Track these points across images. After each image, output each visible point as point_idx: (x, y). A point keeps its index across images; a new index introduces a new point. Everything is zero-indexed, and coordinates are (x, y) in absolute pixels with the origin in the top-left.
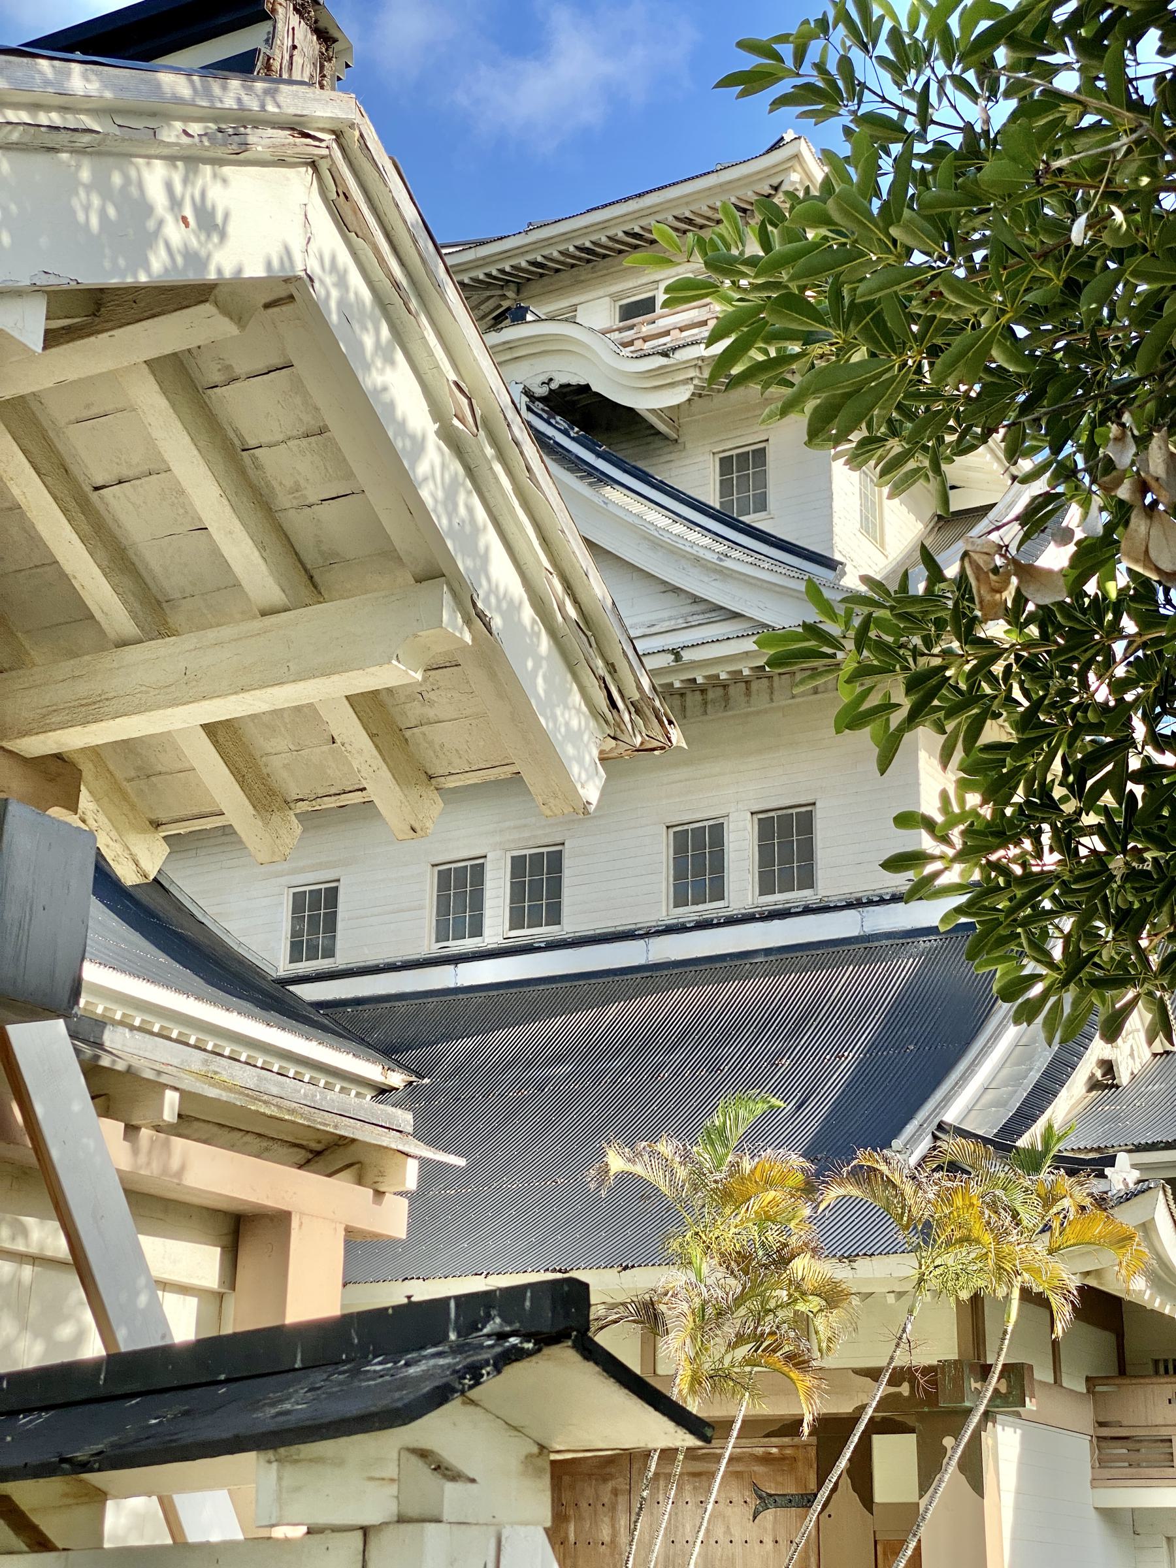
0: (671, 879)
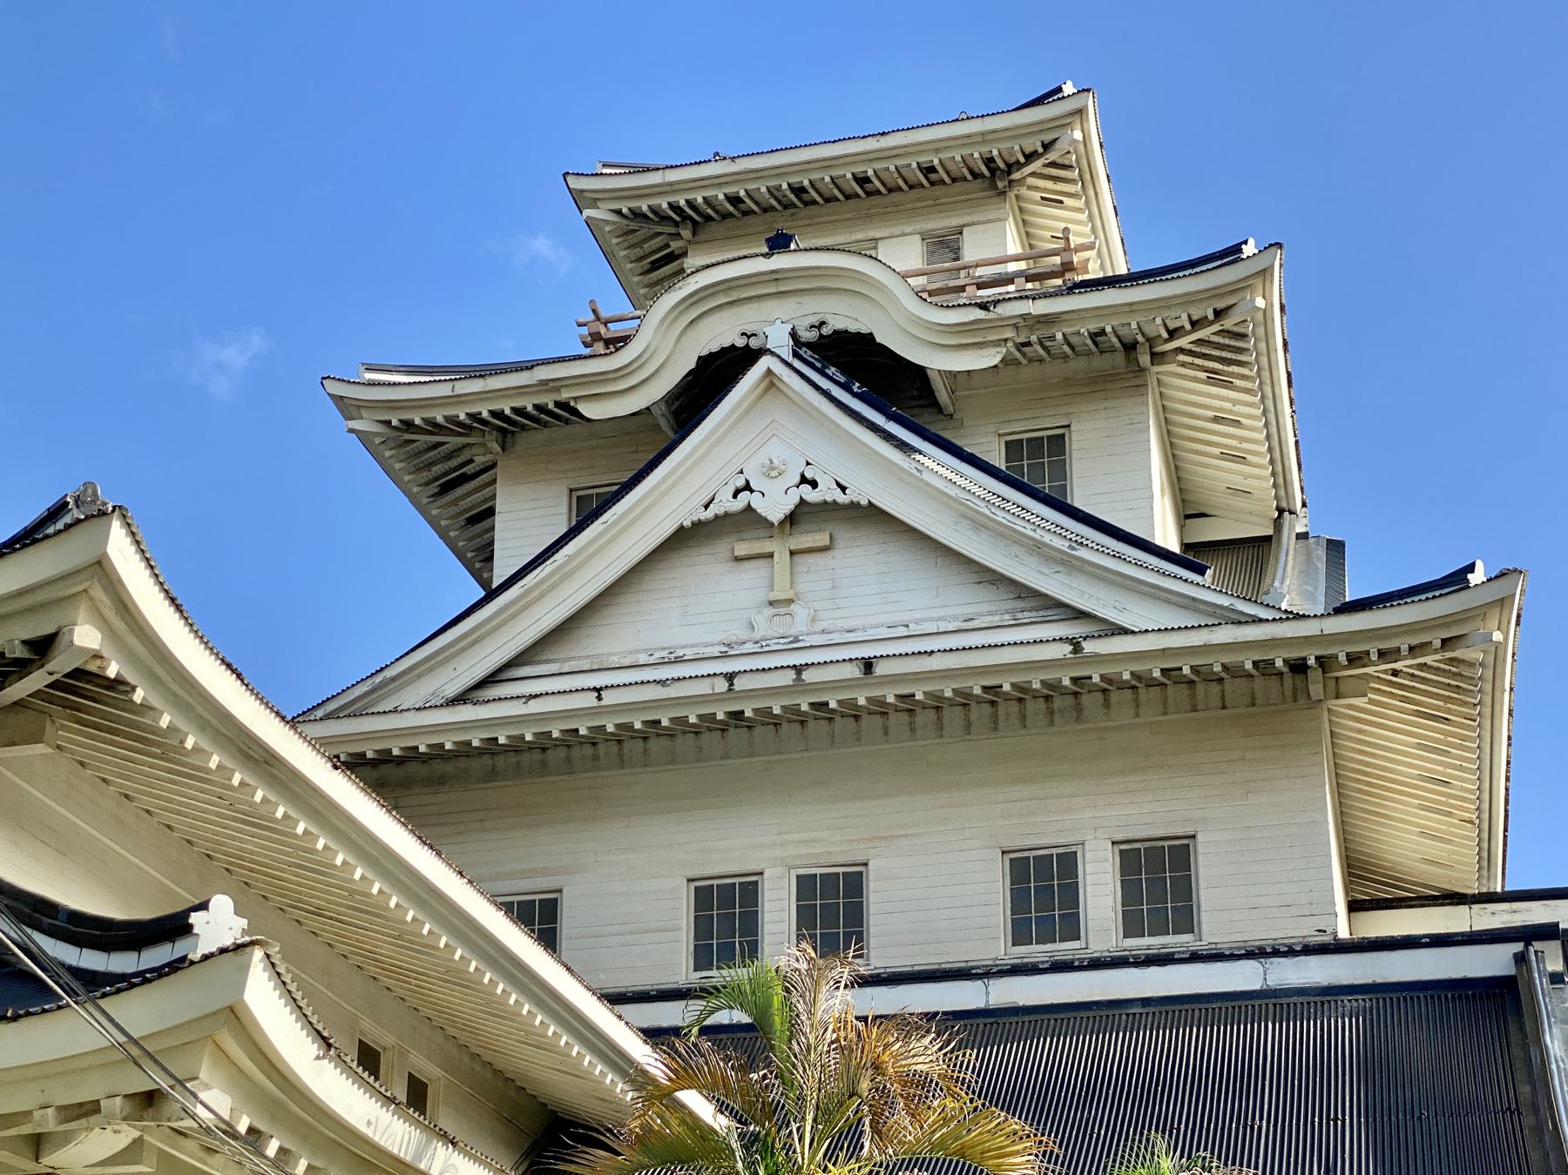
0: (1009, 912)
